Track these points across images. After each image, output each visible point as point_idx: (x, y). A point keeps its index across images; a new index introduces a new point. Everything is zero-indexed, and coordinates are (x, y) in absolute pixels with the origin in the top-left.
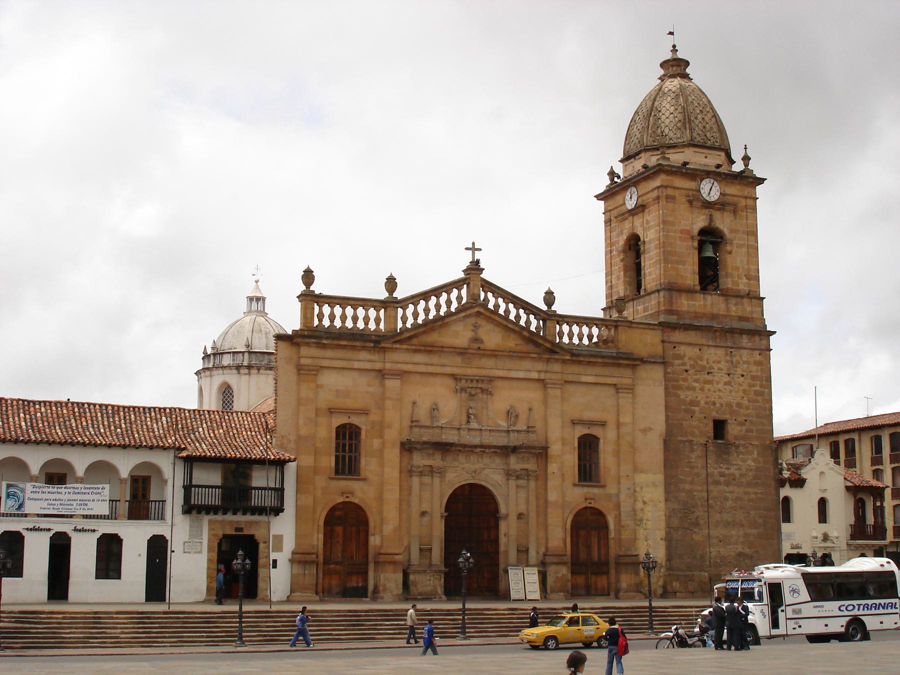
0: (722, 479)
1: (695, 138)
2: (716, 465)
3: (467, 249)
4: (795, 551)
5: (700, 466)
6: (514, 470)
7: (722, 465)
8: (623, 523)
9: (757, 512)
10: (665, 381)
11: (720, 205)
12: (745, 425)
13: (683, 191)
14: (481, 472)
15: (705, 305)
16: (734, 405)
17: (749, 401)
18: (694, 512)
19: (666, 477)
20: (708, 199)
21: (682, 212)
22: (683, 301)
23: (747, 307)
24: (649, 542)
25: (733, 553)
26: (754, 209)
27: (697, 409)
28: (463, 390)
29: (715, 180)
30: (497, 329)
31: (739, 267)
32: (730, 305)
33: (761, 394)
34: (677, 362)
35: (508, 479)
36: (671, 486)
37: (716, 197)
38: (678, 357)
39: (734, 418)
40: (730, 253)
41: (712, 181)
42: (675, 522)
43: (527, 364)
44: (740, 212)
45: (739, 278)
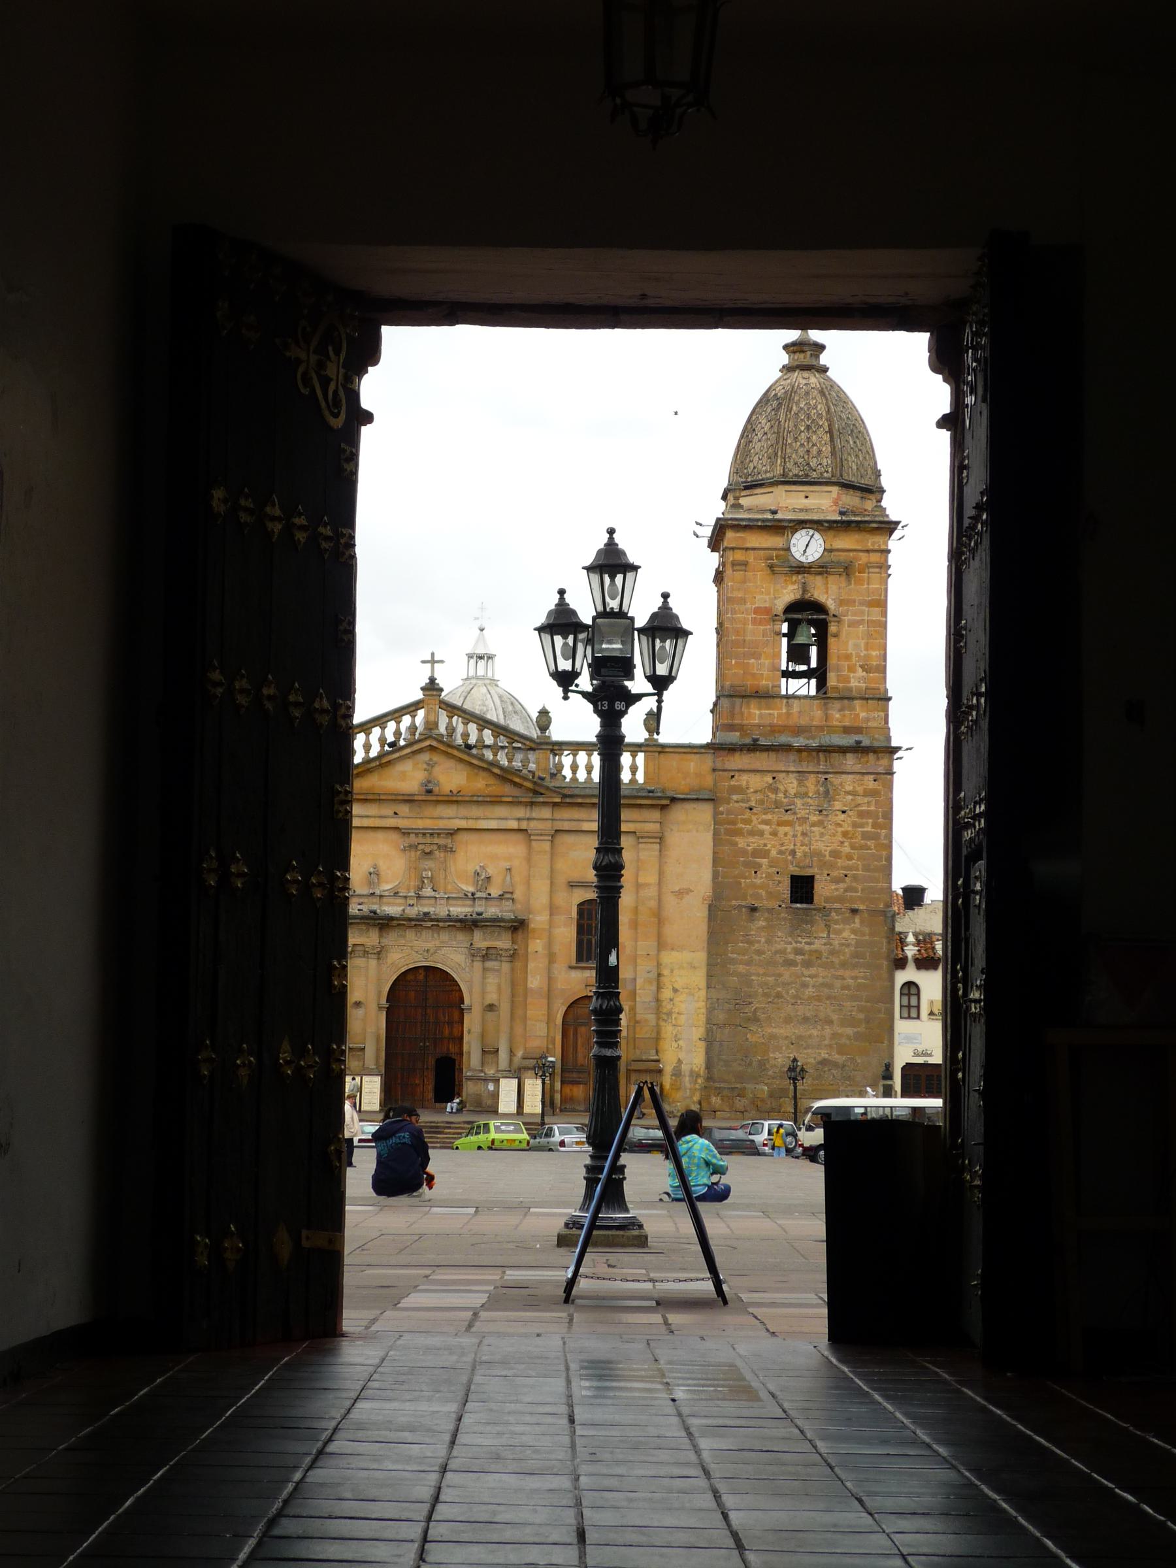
0: (799, 958)
1: (790, 471)
2: (790, 939)
3: (424, 662)
4: (920, 1060)
5: (763, 940)
6: (479, 949)
7: (800, 939)
8: (638, 1017)
9: (855, 1004)
10: (714, 824)
11: (821, 569)
12: (843, 881)
13: (762, 552)
14: (435, 952)
15: (788, 714)
16: (827, 854)
17: (853, 847)
18: (750, 1003)
19: (710, 954)
20: (803, 559)
21: (759, 583)
22: (752, 711)
23: (862, 712)
24: (681, 1043)
25: (812, 1061)
26: (884, 567)
27: (764, 861)
28: (413, 847)
29: (817, 530)
30: (460, 766)
32: (830, 712)
33: (875, 837)
34: (735, 797)
35: (473, 961)
36: (716, 968)
37: (817, 556)
38: (739, 790)
39: (826, 872)
40: (836, 636)
41: (811, 532)
42: (721, 1017)
43: (501, 811)
44: (857, 574)
45: (851, 669)
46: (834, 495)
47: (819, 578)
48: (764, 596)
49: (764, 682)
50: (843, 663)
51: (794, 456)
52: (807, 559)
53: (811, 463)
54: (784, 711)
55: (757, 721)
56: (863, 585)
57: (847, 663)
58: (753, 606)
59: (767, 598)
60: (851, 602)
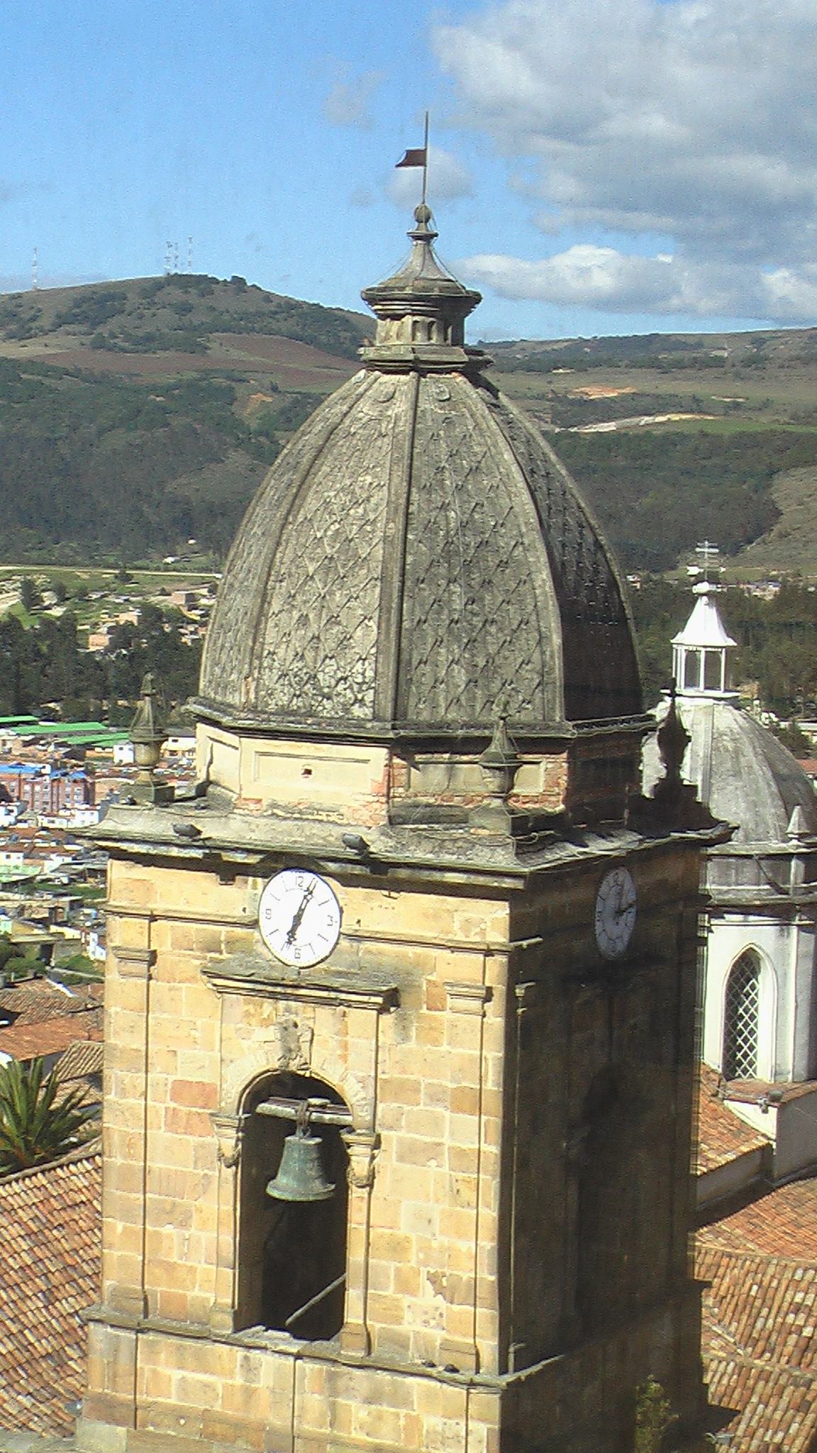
15: (249, 1393)
20: (288, 955)
31: (407, 1239)
45: (406, 1286)
47: (324, 1013)
49: (195, 1293)
50: (383, 1262)
51: (281, 652)
53: (320, 676)
54: (239, 1381)
55: (173, 1401)
56: (436, 1043)
57: (393, 1265)
58: (172, 1078)
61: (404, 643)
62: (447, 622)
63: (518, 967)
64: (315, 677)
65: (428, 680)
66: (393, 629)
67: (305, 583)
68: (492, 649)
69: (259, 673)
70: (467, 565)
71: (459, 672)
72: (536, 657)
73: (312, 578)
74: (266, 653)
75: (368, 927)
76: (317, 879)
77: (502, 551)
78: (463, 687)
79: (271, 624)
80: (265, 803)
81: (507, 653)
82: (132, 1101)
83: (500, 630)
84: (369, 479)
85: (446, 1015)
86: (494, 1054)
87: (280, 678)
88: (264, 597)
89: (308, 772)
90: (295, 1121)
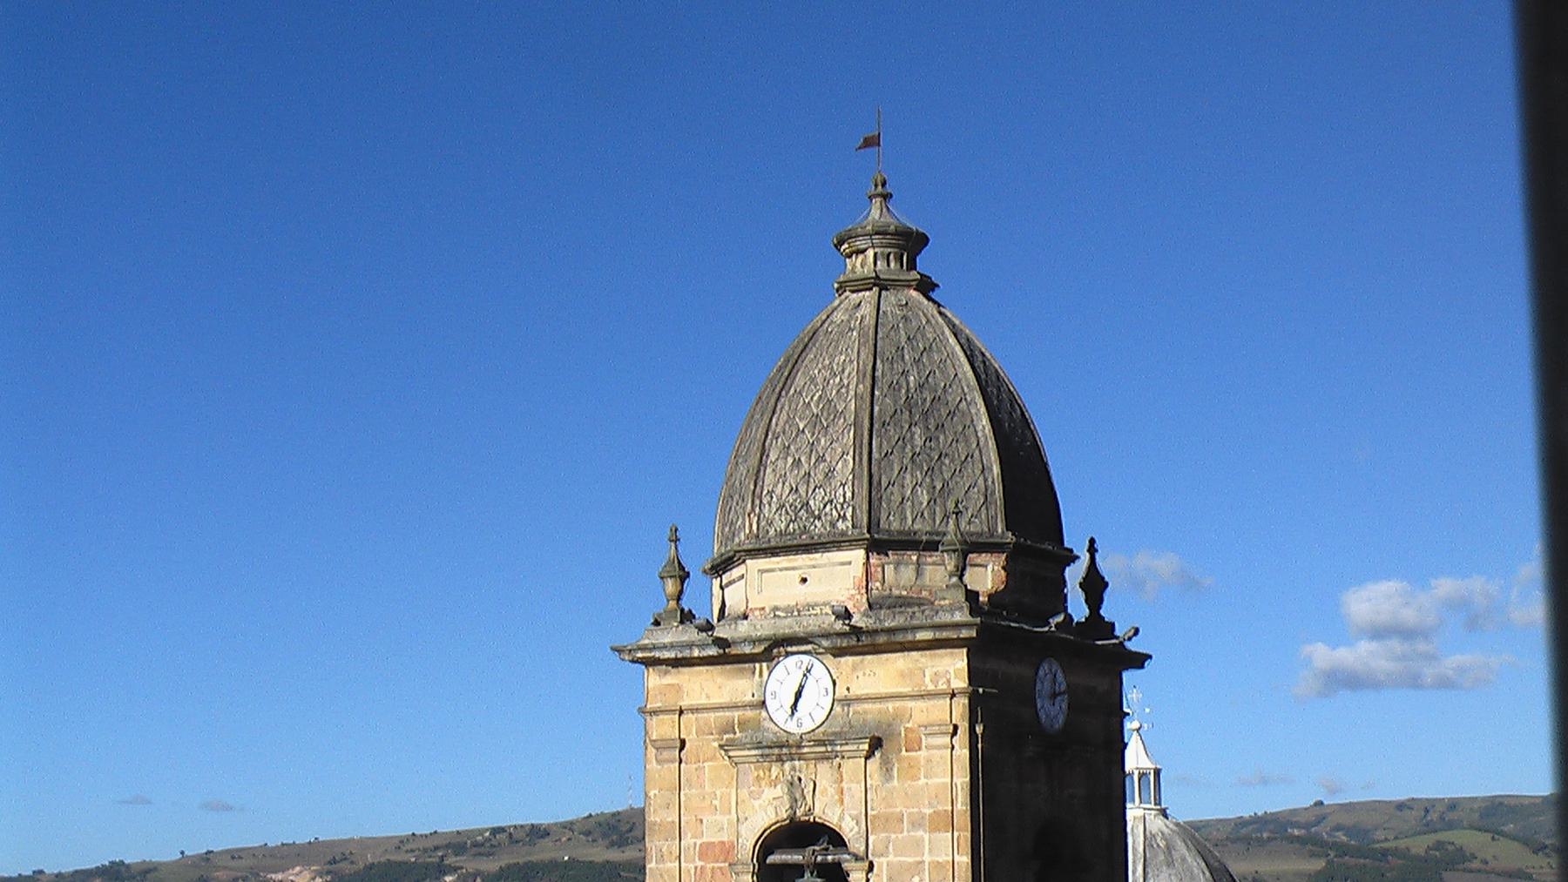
11: (826, 744)
13: (712, 715)
20: (792, 727)
21: (708, 788)
37: (820, 716)
44: (904, 752)
46: (858, 570)
47: (824, 767)
48: (718, 817)
51: (778, 490)
52: (800, 725)
56: (916, 778)
58: (699, 842)
59: (724, 819)
60: (892, 821)
61: (875, 469)
62: (910, 455)
63: (977, 705)
64: (808, 503)
65: (897, 498)
66: (865, 458)
67: (797, 436)
68: (947, 476)
69: (760, 508)
70: (925, 415)
71: (922, 492)
72: (981, 481)
73: (803, 431)
74: (765, 493)
75: (857, 691)
76: (812, 658)
77: (950, 404)
78: (925, 504)
79: (769, 470)
80: (767, 610)
81: (958, 479)
82: (669, 865)
83: (952, 461)
84: (843, 357)
85: (923, 753)
86: (963, 779)
87: (777, 510)
88: (764, 452)
89: (804, 580)
90: (802, 866)
